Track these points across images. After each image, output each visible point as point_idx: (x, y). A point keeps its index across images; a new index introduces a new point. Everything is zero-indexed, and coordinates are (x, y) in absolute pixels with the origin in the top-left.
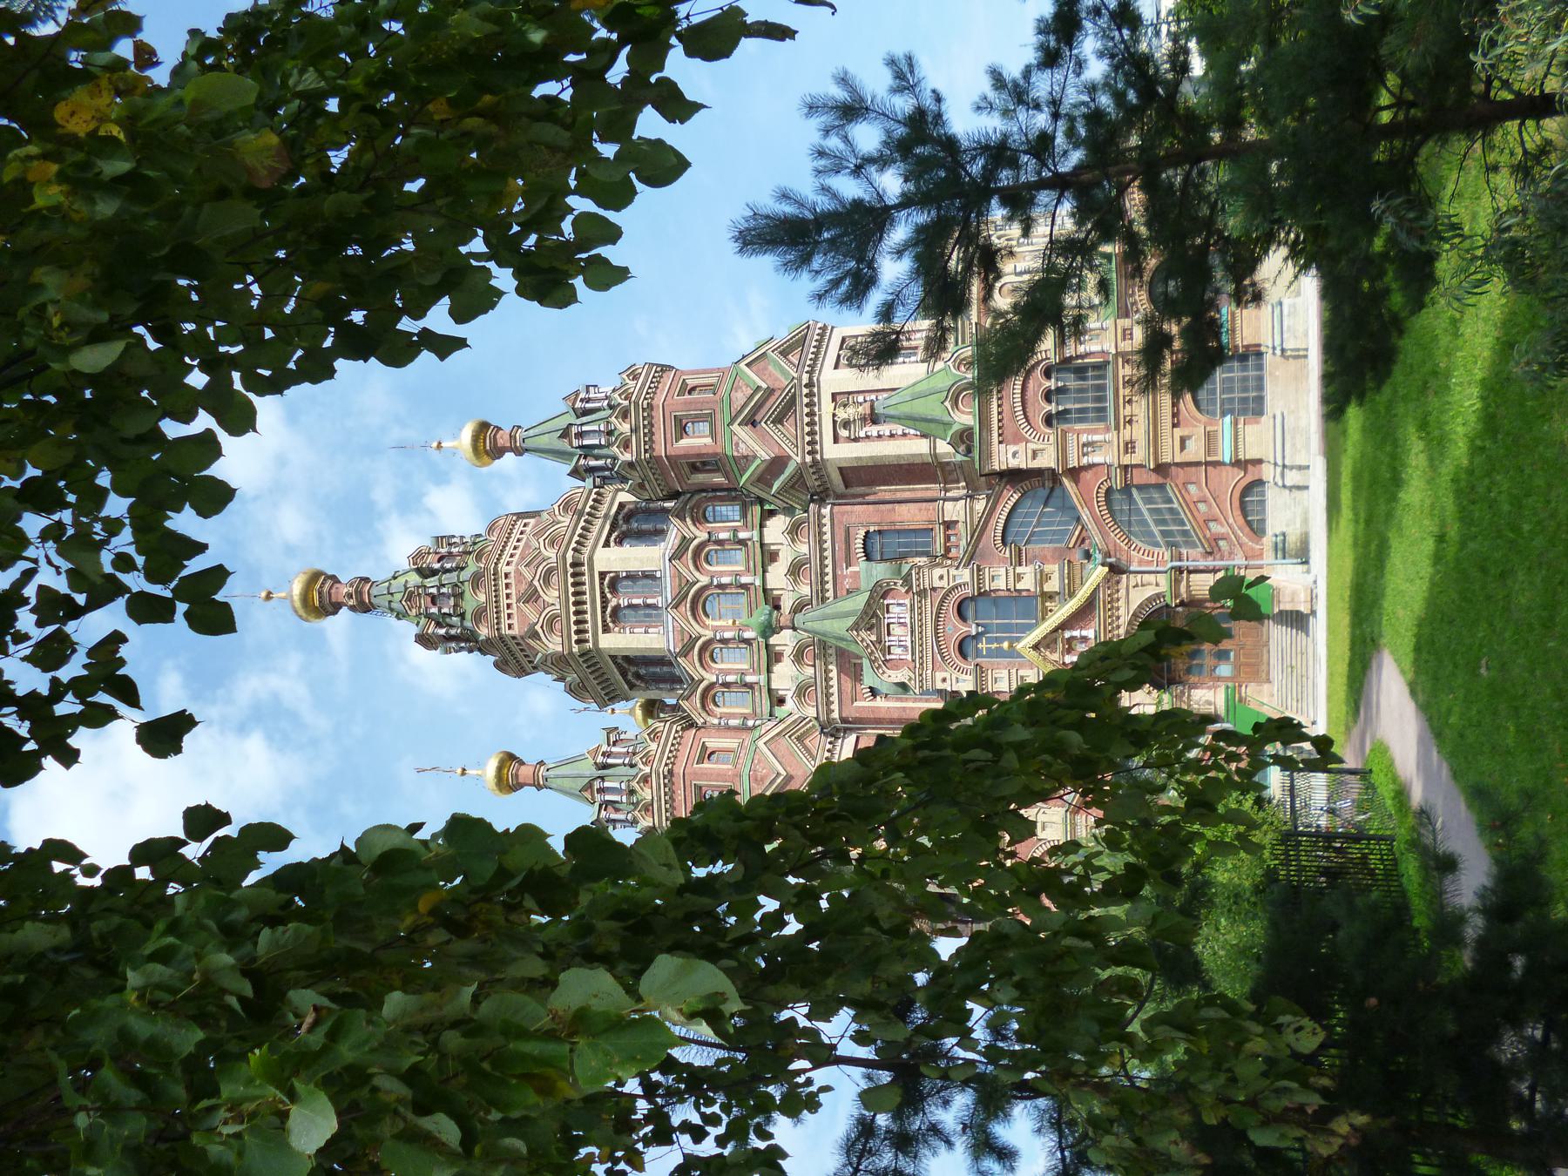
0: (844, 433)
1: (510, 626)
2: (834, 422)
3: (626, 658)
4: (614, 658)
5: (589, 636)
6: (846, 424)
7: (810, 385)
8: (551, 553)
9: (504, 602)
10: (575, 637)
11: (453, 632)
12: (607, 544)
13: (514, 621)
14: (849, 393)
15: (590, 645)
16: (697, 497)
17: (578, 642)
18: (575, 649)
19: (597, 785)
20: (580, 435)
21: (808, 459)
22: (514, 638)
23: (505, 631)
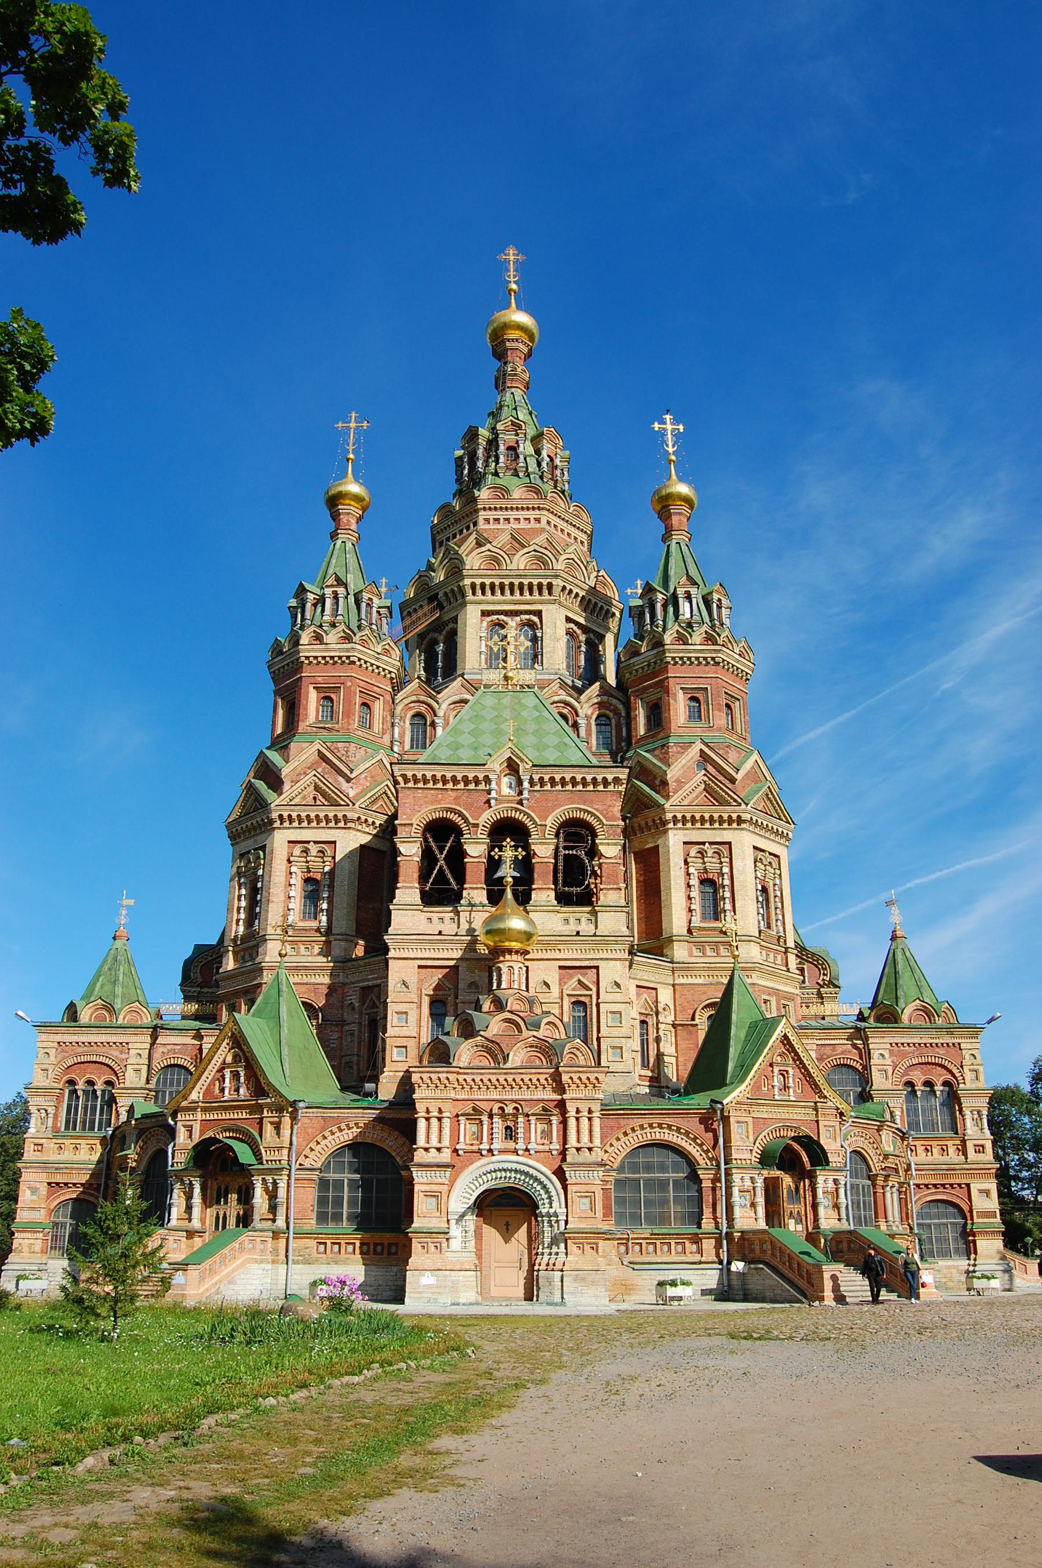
0: (694, 851)
1: (487, 521)
2: (704, 843)
3: (454, 633)
4: (455, 620)
5: (479, 597)
6: (702, 854)
7: (740, 821)
8: (560, 565)
9: (512, 515)
10: (478, 581)
11: (480, 464)
13: (492, 526)
14: (731, 859)
15: (470, 597)
16: (621, 707)
17: (473, 586)
18: (467, 582)
20: (688, 597)
21: (669, 816)
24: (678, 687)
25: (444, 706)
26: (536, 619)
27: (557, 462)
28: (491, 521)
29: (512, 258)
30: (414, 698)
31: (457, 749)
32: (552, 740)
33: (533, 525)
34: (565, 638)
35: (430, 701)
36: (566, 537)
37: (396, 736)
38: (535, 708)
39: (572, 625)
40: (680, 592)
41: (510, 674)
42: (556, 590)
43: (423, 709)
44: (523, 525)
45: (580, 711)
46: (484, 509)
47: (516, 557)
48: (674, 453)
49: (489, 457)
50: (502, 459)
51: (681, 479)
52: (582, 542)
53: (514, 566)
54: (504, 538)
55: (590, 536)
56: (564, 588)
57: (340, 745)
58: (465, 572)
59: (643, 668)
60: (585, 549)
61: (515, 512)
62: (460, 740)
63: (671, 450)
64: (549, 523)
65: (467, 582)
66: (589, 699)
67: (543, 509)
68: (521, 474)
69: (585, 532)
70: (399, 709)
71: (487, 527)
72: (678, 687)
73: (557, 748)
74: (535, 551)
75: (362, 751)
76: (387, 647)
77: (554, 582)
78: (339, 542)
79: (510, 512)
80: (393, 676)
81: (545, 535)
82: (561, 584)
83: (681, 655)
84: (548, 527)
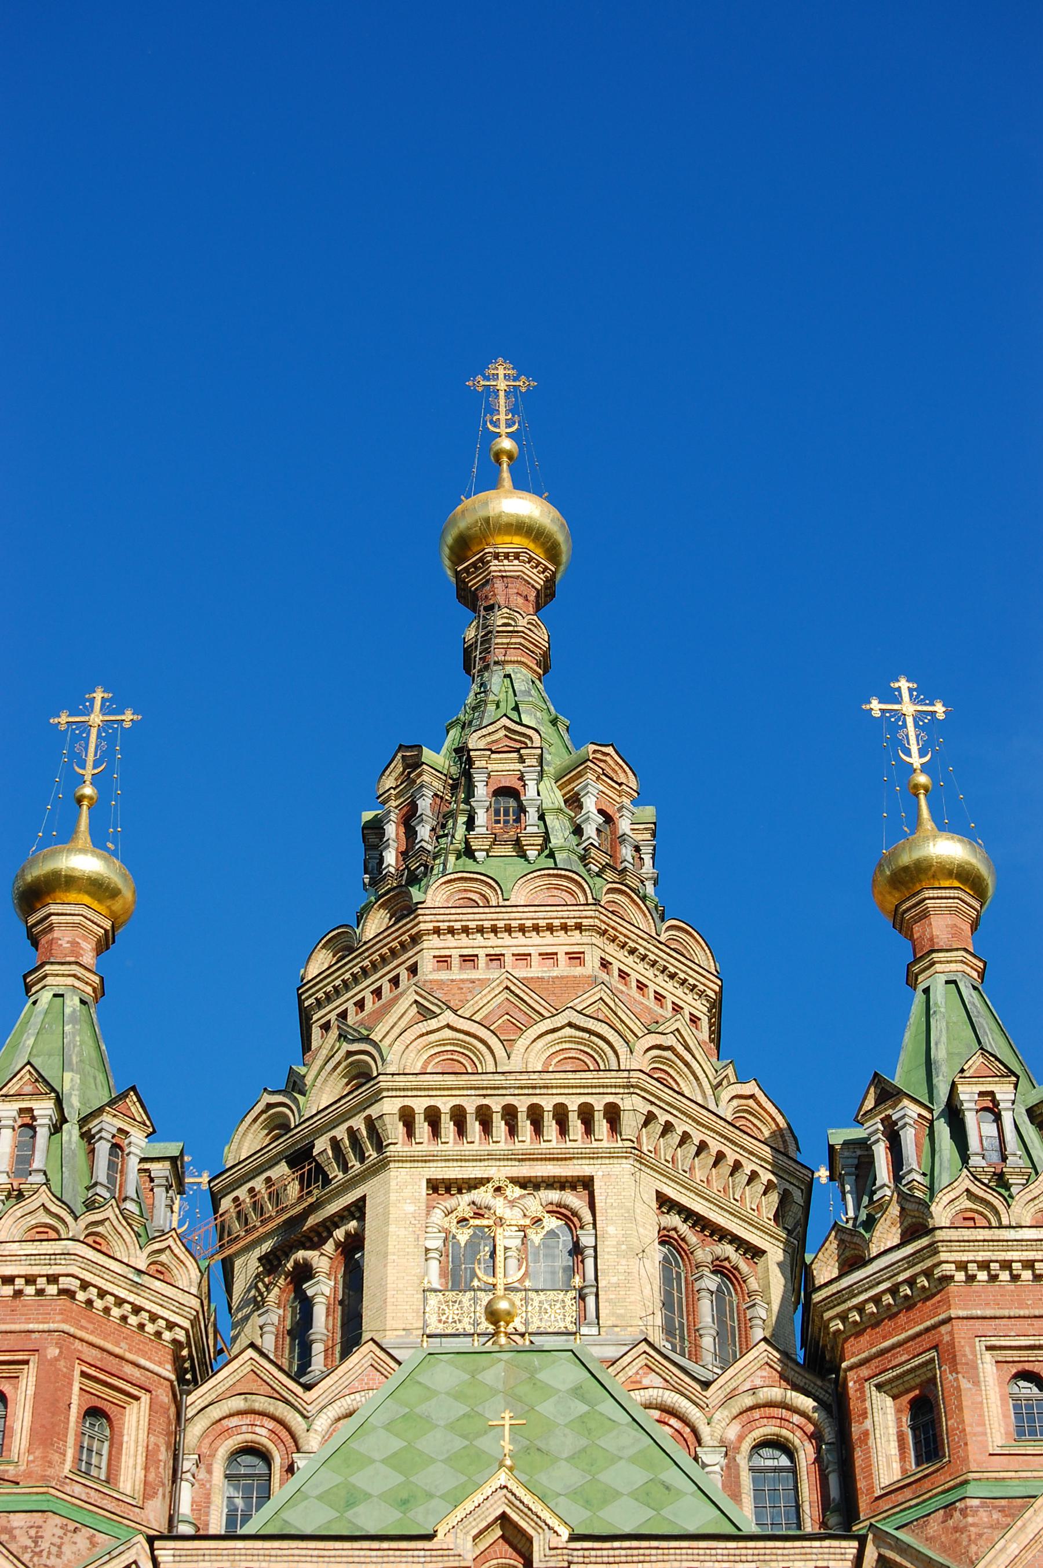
1: (443, 961)
10: (419, 1105)
11: (424, 832)
12: (665, 1203)
13: (457, 973)
18: (390, 1106)
19: (44, 1109)
22: (413, 970)
23: (432, 944)
24: (980, 1345)
25: (322, 1423)
26: (575, 1200)
27: (624, 826)
28: (456, 962)
29: (502, 385)
30: (238, 1403)
31: (350, 1504)
32: (625, 1476)
33: (564, 968)
34: (657, 1253)
35: (281, 1410)
36: (651, 1003)
37: (185, 1508)
38: (577, 1392)
39: (674, 1220)
40: (968, 1094)
41: (503, 1305)
42: (630, 1124)
43: (262, 1434)
44: (537, 969)
45: (705, 1431)
46: (437, 931)
47: (522, 1043)
48: (925, 768)
49: (452, 815)
50: (481, 818)
51: (947, 824)
52: (694, 1020)
53: (516, 1063)
54: (488, 1001)
55: (716, 1007)
56: (650, 1118)
57: (18, 1521)
58: (384, 1082)
59: (876, 1300)
60: (704, 1035)
61: (520, 939)
62: (361, 1480)
63: (916, 761)
64: (605, 964)
65: (390, 1106)
66: (730, 1397)
67: (593, 928)
68: (532, 854)
69: (701, 994)
70: (194, 1431)
71: (444, 975)
72: (980, 1345)
73: (642, 1496)
74: (570, 1025)
75: (81, 1539)
76: (163, 1258)
77: (626, 1103)
78: (46, 997)
79: (506, 939)
80: (181, 1336)
81: (597, 993)
82: (645, 1108)
83: (981, 1256)
84: (605, 977)
